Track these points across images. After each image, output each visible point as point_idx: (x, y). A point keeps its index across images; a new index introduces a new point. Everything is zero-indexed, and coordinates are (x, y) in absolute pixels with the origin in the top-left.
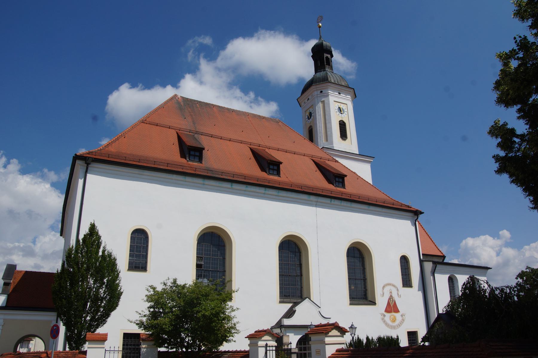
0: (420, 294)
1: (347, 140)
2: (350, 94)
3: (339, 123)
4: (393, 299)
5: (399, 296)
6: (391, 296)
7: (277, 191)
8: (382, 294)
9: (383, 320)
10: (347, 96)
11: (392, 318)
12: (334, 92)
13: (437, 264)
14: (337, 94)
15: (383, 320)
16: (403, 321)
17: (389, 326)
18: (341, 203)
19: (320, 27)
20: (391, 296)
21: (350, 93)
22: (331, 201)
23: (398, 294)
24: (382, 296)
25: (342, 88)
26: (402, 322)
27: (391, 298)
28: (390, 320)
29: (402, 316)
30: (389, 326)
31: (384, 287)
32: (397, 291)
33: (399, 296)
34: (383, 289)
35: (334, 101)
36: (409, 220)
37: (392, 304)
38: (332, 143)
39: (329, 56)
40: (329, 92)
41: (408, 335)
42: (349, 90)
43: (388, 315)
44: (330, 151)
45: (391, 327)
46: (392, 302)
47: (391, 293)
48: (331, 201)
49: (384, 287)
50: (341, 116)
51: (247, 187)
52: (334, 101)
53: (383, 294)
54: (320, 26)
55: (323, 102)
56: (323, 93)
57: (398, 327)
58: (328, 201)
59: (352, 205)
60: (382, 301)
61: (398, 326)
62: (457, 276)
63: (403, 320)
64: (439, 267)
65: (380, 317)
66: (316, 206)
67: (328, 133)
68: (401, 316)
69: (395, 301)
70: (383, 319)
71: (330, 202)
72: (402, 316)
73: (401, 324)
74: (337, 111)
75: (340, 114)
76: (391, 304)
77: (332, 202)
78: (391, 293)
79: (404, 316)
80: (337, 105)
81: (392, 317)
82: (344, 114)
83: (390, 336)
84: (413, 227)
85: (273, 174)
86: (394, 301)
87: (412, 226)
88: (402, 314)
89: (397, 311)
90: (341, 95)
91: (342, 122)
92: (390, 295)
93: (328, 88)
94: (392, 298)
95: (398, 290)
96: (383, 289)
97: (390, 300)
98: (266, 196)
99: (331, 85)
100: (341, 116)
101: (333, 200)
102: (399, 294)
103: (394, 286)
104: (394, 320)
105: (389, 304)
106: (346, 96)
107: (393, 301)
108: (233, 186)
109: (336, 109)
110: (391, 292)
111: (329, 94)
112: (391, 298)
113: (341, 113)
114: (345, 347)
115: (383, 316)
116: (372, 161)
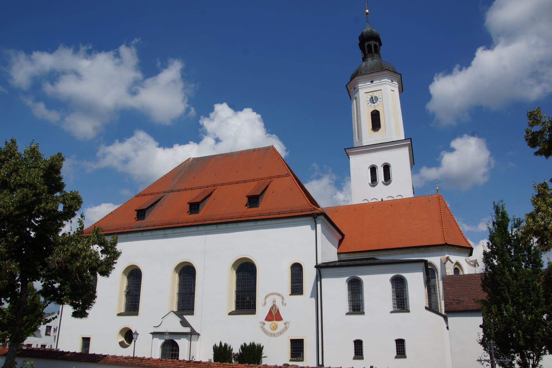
0: (313, 300)
1: (380, 130)
2: (386, 76)
3: (371, 115)
6: (274, 305)
7: (172, 230)
8: (264, 303)
9: (262, 328)
10: (382, 81)
11: (273, 326)
13: (319, 268)
14: (370, 83)
15: (262, 328)
16: (285, 329)
17: (269, 334)
18: (227, 226)
19: (367, 14)
20: (274, 305)
22: (217, 227)
23: (283, 303)
24: (263, 305)
26: (284, 330)
27: (274, 306)
28: (271, 328)
29: (286, 324)
30: (269, 334)
34: (266, 299)
35: (365, 93)
36: (308, 225)
37: (274, 313)
38: (361, 140)
39: (373, 43)
40: (359, 85)
41: (291, 343)
43: (268, 323)
44: (353, 150)
45: (270, 335)
46: (274, 310)
47: (274, 302)
48: (217, 227)
50: (374, 105)
51: (151, 233)
52: (365, 93)
53: (265, 303)
54: (368, 13)
55: (356, 98)
56: (356, 88)
57: (278, 334)
58: (214, 227)
60: (262, 309)
62: (363, 278)
63: (286, 328)
64: (323, 271)
65: (259, 325)
66: (206, 234)
67: (359, 129)
68: (284, 324)
69: (278, 309)
70: (262, 327)
71: (216, 227)
72: (285, 324)
73: (283, 331)
74: (369, 102)
75: (373, 105)
76: (273, 313)
77: (218, 227)
78: (275, 302)
79: (288, 324)
80: (369, 96)
82: (378, 102)
83: (243, 345)
84: (314, 230)
85: (194, 213)
86: (277, 310)
87: (312, 230)
88: (286, 322)
89: (279, 318)
90: (374, 82)
91: (375, 112)
92: (273, 304)
93: (358, 82)
95: (283, 298)
96: (266, 299)
100: (374, 105)
101: (218, 226)
102: (284, 303)
103: (279, 295)
104: (275, 328)
105: (270, 312)
106: (381, 80)
107: (276, 309)
108: (143, 234)
109: (368, 101)
111: (359, 88)
112: (274, 306)
113: (374, 103)
114: (240, 351)
115: (262, 324)
116: (409, 143)
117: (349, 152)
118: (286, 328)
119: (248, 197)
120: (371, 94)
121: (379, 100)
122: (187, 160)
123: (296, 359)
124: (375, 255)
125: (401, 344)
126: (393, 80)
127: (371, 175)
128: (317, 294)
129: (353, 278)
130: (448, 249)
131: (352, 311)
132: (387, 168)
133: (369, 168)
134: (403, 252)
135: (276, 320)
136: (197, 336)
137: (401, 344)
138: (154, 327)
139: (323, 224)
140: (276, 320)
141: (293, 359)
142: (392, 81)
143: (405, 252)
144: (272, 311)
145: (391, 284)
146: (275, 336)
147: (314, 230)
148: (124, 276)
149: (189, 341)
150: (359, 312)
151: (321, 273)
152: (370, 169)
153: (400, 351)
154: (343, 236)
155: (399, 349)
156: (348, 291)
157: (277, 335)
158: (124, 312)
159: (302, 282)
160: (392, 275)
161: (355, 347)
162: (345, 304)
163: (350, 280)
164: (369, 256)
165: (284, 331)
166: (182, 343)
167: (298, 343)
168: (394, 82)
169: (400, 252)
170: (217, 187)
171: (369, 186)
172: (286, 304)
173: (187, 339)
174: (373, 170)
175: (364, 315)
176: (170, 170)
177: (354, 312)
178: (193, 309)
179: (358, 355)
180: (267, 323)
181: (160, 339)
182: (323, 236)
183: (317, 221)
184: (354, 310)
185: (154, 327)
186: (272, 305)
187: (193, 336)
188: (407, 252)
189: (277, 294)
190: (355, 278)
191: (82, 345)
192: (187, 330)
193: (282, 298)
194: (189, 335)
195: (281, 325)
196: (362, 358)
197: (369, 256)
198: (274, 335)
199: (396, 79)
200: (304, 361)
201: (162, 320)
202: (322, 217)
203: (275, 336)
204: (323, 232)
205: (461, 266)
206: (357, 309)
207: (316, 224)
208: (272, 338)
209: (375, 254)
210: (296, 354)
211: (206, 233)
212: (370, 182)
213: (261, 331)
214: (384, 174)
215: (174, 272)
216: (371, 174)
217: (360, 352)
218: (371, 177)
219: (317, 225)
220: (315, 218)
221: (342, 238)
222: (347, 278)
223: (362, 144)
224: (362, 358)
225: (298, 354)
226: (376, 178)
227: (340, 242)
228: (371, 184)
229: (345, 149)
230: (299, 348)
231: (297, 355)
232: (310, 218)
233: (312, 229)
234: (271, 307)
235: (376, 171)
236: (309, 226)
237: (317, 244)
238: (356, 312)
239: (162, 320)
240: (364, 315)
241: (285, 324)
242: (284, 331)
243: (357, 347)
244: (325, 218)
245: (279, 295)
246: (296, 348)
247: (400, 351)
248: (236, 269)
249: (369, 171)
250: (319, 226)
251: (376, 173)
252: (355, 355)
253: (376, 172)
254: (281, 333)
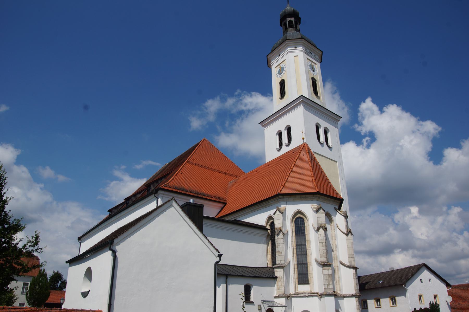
10: (286, 51)
12: (276, 59)
21: (287, 45)
25: (279, 49)
35: (276, 67)
42: (284, 44)
74: (278, 74)
80: (278, 69)
99: (270, 56)
100: (281, 75)
120: (279, 66)
121: (285, 69)
124: (236, 217)
126: (295, 46)
127: (279, 141)
130: (283, 199)
132: (289, 129)
133: (277, 135)
134: (252, 210)
142: (296, 48)
143: (253, 209)
164: (232, 218)
168: (298, 48)
169: (250, 210)
174: (280, 134)
188: (254, 209)
197: (232, 218)
199: (301, 45)
205: (305, 215)
209: (236, 216)
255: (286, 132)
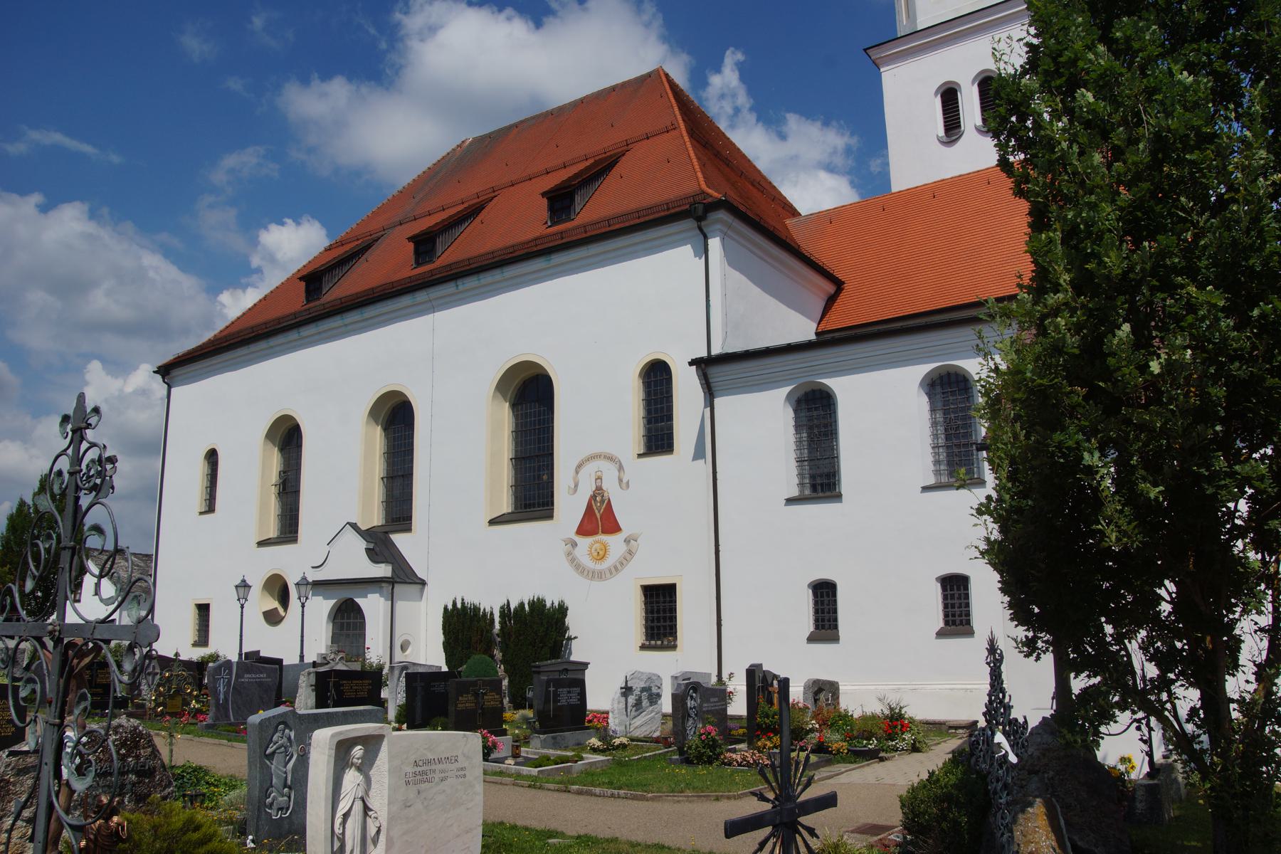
4: (603, 496)
5: (624, 485)
6: (599, 488)
9: (570, 557)
13: (703, 366)
15: (570, 557)
16: (628, 557)
17: (586, 573)
18: (479, 280)
20: (599, 488)
23: (620, 480)
27: (598, 493)
28: (591, 554)
30: (586, 573)
31: (579, 466)
32: (619, 471)
33: (623, 484)
34: (577, 472)
37: (599, 512)
41: (645, 596)
43: (584, 542)
44: (891, 49)
47: (599, 480)
48: (457, 286)
49: (579, 467)
53: (576, 486)
57: (611, 573)
59: (505, 274)
61: (613, 569)
63: (630, 553)
64: (716, 372)
65: (563, 548)
66: (433, 309)
69: (609, 501)
70: (569, 554)
72: (627, 541)
73: (622, 564)
76: (596, 511)
81: (597, 545)
84: (700, 258)
89: (612, 526)
94: (599, 494)
95: (621, 468)
96: (577, 472)
97: (595, 500)
98: (349, 328)
102: (625, 481)
103: (610, 458)
104: (601, 556)
105: (589, 511)
107: (602, 501)
110: (599, 478)
112: (598, 493)
115: (569, 545)
117: (878, 56)
118: (630, 553)
119: (550, 195)
122: (458, 146)
123: (659, 642)
125: (959, 589)
127: (944, 114)
128: (707, 447)
129: (808, 389)
131: (807, 492)
135: (605, 532)
136: (420, 586)
137: (959, 589)
138: (313, 567)
139: (730, 237)
140: (603, 532)
141: (653, 642)
144: (595, 508)
145: (925, 399)
146: (601, 578)
147: (700, 258)
148: (271, 445)
149: (386, 600)
150: (828, 494)
151: (711, 381)
152: (939, 96)
153: (954, 615)
154: (839, 284)
155: (953, 606)
156: (796, 430)
157: (608, 575)
158: (276, 536)
159: (670, 418)
160: (924, 369)
161: (816, 603)
162: (787, 478)
163: (800, 393)
165: (625, 562)
166: (373, 606)
167: (664, 597)
170: (499, 192)
171: (940, 145)
172: (628, 483)
173: (381, 596)
174: (949, 96)
175: (841, 502)
176: (414, 176)
177: (814, 495)
178: (410, 518)
179: (823, 627)
180: (580, 540)
181: (325, 598)
182: (736, 275)
183: (705, 230)
184: (814, 488)
185: (313, 567)
186: (594, 489)
187: (398, 588)
189: (605, 457)
190: (815, 388)
191: (197, 622)
192: (383, 570)
193: (617, 465)
194: (384, 585)
195: (614, 542)
196: (835, 639)
198: (599, 576)
200: (678, 648)
201: (327, 548)
202: (722, 215)
203: (601, 578)
204: (732, 260)
206: (822, 485)
207: (706, 238)
208: (596, 584)
210: (658, 628)
211: (432, 308)
212: (941, 132)
213: (567, 564)
214: (981, 104)
215: (367, 423)
216: (944, 110)
217: (829, 621)
218: (945, 118)
219: (710, 241)
220: (700, 219)
221: (836, 292)
222: (789, 389)
223: (916, 26)
224: (835, 639)
225: (665, 627)
226: (959, 118)
227: (831, 301)
228: (945, 139)
229: (865, 50)
230: (664, 611)
231: (662, 631)
232: (689, 224)
233: (695, 256)
234: (591, 497)
235: (957, 99)
236: (689, 246)
237: (711, 299)
238: (821, 494)
239: (327, 548)
240: (841, 502)
241: (627, 541)
242: (625, 562)
243: (822, 603)
244: (732, 218)
245: (610, 458)
246: (658, 612)
247: (954, 615)
248: (509, 396)
249: (938, 102)
250: (715, 244)
251: (958, 106)
252: (817, 627)
253: (958, 103)
254: (616, 569)
255: (975, 89)
